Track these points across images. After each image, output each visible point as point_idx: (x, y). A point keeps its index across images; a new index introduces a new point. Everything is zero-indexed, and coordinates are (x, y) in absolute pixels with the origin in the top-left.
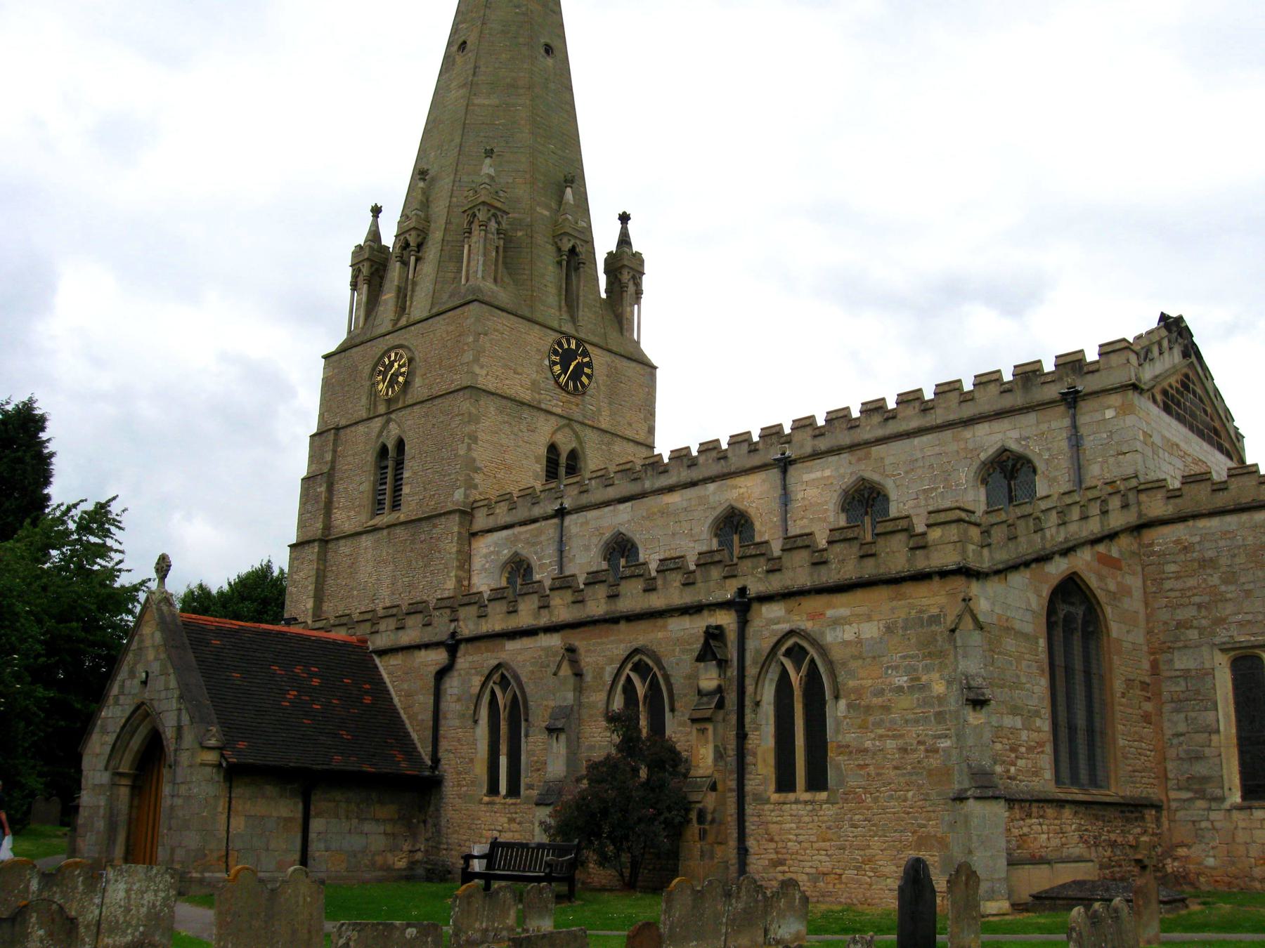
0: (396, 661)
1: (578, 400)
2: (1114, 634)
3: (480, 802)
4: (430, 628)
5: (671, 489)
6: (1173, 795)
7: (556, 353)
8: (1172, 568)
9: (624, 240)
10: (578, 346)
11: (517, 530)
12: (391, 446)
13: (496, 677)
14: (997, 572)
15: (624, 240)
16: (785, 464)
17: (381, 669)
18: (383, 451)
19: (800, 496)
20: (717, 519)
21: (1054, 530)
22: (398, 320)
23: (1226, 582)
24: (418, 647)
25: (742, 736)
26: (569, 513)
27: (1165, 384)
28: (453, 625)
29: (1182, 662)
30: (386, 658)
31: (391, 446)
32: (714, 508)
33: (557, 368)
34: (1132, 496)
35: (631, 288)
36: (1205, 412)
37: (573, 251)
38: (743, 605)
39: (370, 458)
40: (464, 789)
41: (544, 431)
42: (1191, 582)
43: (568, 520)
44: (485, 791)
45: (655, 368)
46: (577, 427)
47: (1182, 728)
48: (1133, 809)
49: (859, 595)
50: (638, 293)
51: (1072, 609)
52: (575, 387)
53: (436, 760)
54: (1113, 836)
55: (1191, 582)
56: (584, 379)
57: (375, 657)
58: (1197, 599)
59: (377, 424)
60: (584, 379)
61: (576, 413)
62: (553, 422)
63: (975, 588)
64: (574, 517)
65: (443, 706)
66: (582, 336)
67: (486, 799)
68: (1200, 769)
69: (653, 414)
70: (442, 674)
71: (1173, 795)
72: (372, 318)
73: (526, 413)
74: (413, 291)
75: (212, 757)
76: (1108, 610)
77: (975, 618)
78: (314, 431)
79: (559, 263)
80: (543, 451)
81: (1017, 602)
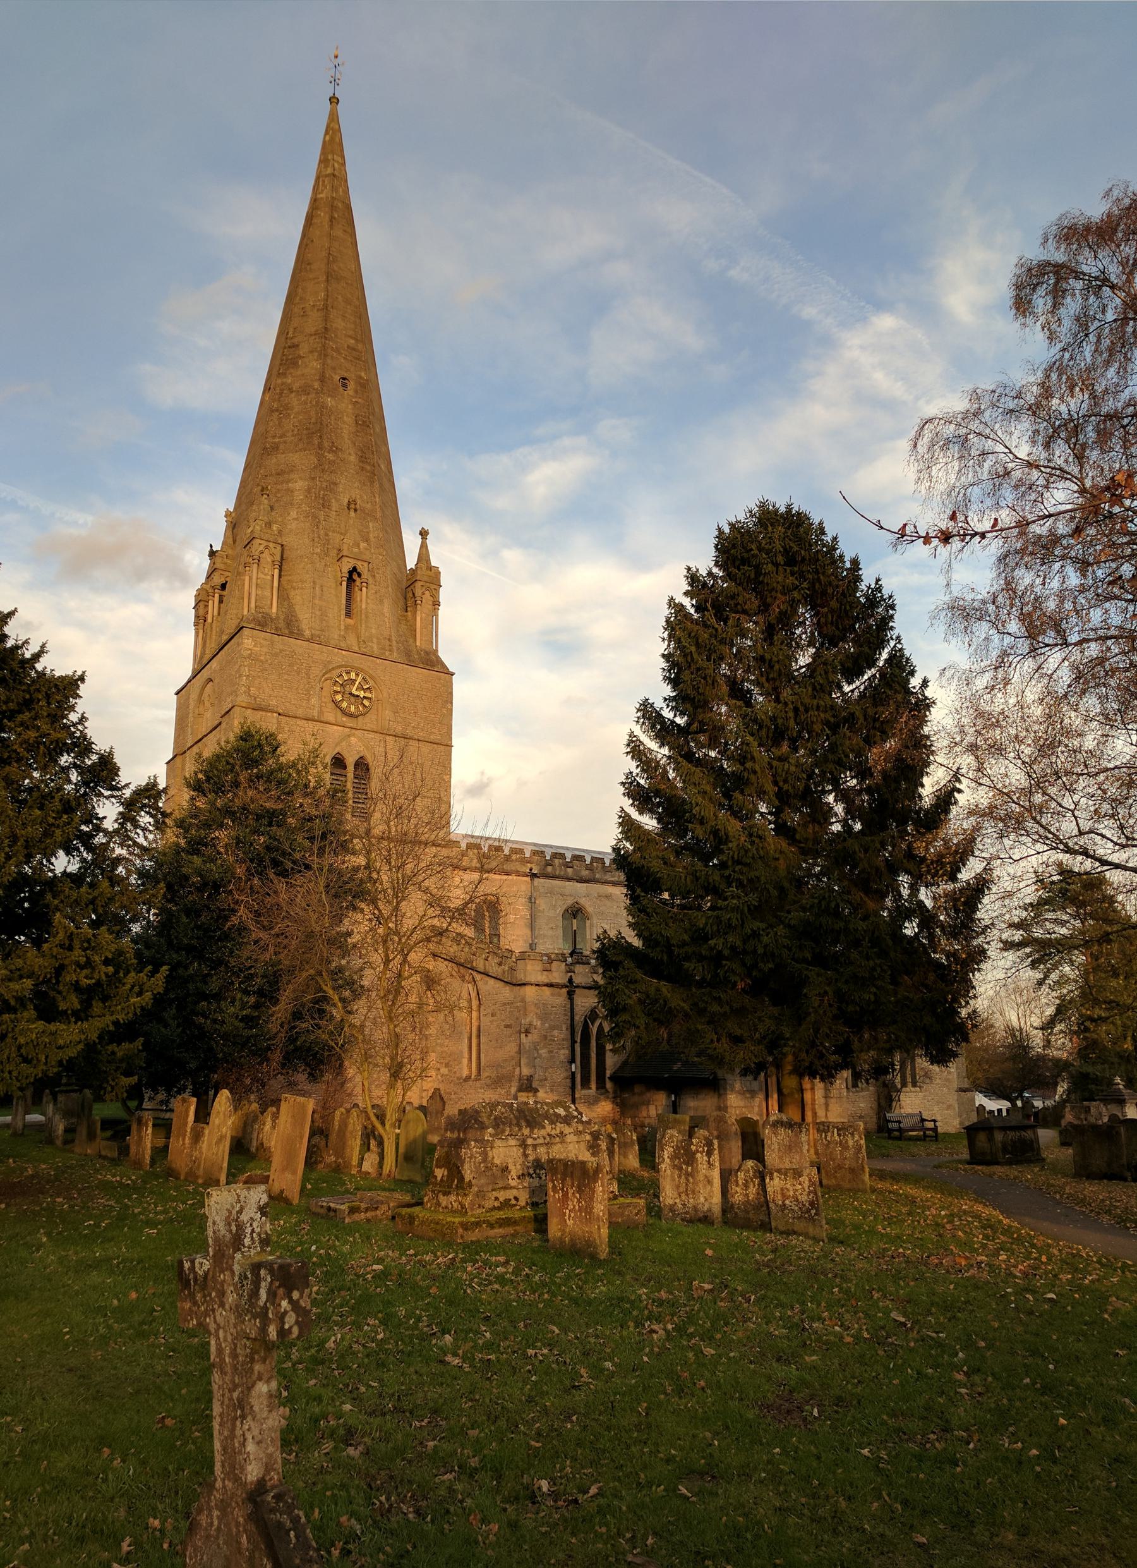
64: (542, 880)
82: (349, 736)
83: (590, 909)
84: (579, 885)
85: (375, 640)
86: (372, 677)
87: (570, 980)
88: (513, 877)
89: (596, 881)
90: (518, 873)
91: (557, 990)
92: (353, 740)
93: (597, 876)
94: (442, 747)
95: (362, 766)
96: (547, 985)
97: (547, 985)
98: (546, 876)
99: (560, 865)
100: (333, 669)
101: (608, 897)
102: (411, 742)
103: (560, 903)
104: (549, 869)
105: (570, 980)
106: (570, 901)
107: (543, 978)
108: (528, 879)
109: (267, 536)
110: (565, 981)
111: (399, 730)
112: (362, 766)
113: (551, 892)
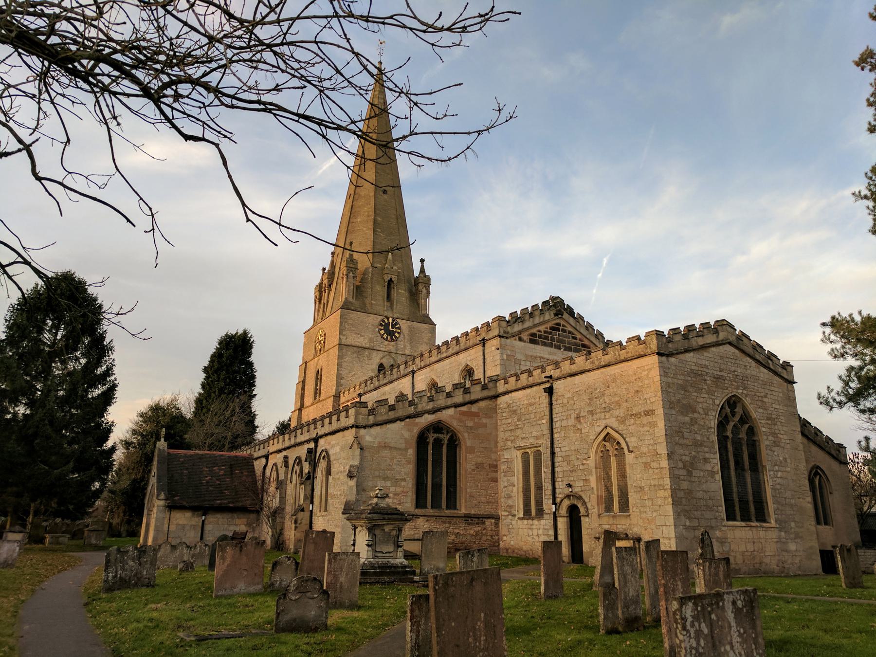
1: (393, 343)
2: (469, 443)
5: (386, 384)
6: (503, 513)
7: (381, 325)
8: (505, 414)
9: (422, 270)
10: (393, 321)
14: (377, 425)
15: (422, 270)
21: (424, 405)
23: (519, 420)
25: (313, 490)
27: (534, 331)
29: (507, 456)
33: (382, 332)
34: (491, 385)
35: (424, 291)
36: (576, 339)
37: (391, 281)
38: (316, 440)
41: (376, 359)
42: (509, 421)
47: (506, 484)
48: (479, 519)
49: (337, 434)
50: (428, 293)
51: (441, 436)
52: (392, 339)
54: (457, 531)
55: (509, 421)
56: (397, 334)
58: (511, 428)
60: (397, 334)
61: (393, 349)
62: (381, 354)
63: (362, 432)
66: (395, 316)
68: (510, 502)
71: (503, 513)
73: (367, 352)
75: (162, 503)
76: (466, 434)
77: (359, 443)
81: (402, 434)
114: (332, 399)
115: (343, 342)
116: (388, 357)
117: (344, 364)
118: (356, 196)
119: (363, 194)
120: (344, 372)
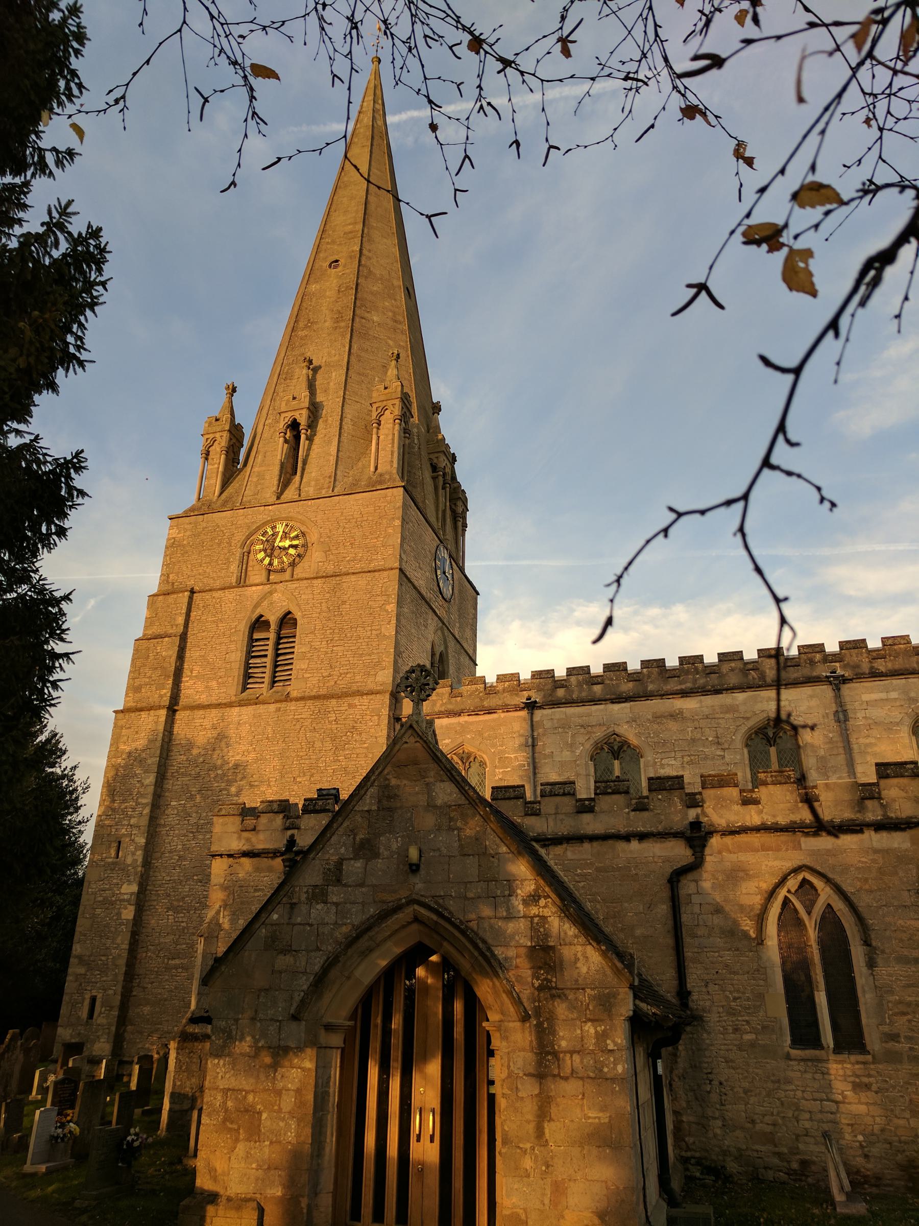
0: (571, 853)
3: (788, 1057)
4: (645, 814)
5: (684, 694)
11: (464, 719)
12: (273, 618)
13: (793, 883)
16: (837, 682)
17: (551, 863)
18: (259, 624)
19: (860, 715)
20: (750, 729)
22: (282, 493)
24: (627, 838)
26: (540, 708)
28: (692, 814)
30: (558, 850)
31: (273, 618)
32: (748, 719)
39: (243, 627)
40: (747, 1037)
43: (539, 714)
44: (789, 1042)
45: (478, 594)
46: (446, 631)
50: (465, 526)
53: (683, 993)
57: (534, 844)
59: (254, 592)
65: (685, 918)
67: (795, 1053)
69: (476, 636)
70: (677, 876)
72: (230, 490)
73: (425, 608)
74: (303, 470)
78: (155, 590)
79: (434, 478)
80: (429, 647)
82: (271, 593)
83: (633, 740)
84: (616, 707)
85: (313, 483)
86: (303, 523)
87: (291, 842)
88: (501, 715)
89: (648, 696)
90: (506, 708)
91: (265, 862)
92: (276, 596)
93: (651, 687)
94: (385, 573)
95: (287, 620)
96: (246, 854)
97: (246, 854)
98: (556, 704)
99: (580, 685)
100: (258, 528)
101: (674, 716)
102: (345, 579)
103: (581, 739)
104: (561, 692)
105: (291, 842)
106: (599, 734)
107: (236, 844)
108: (524, 713)
109: (214, 429)
110: (281, 845)
111: (330, 568)
112: (287, 620)
113: (565, 725)
114: (388, 696)
115: (404, 566)
116: (439, 633)
117: (403, 621)
118: (364, 271)
119: (378, 272)
120: (403, 641)
